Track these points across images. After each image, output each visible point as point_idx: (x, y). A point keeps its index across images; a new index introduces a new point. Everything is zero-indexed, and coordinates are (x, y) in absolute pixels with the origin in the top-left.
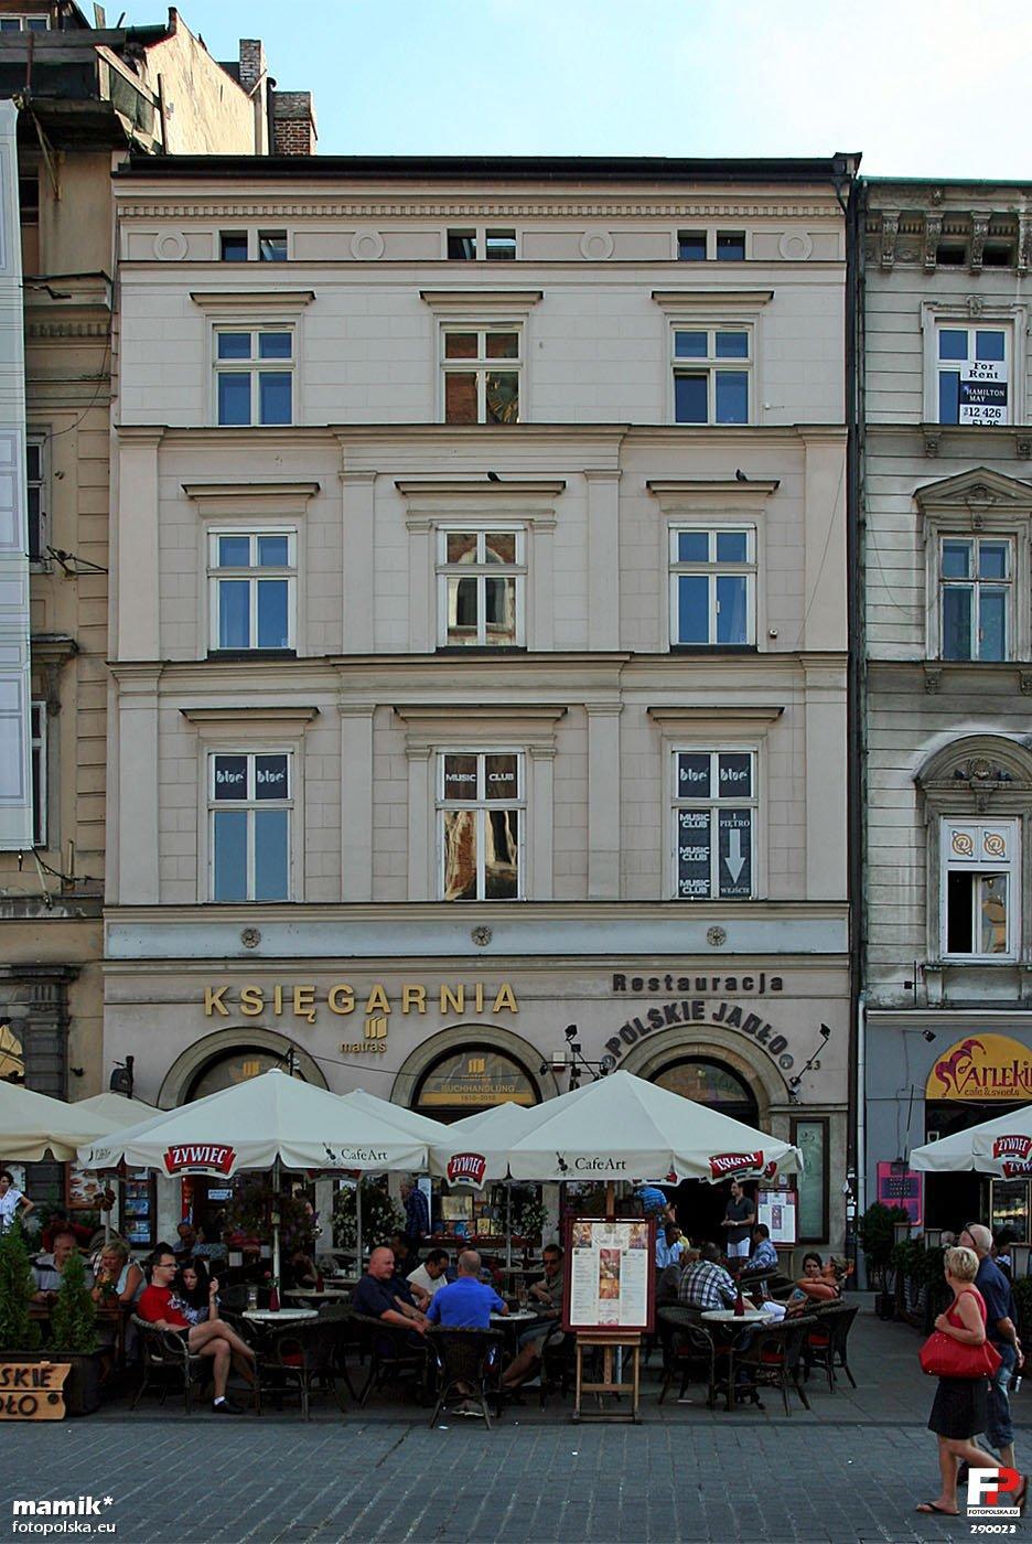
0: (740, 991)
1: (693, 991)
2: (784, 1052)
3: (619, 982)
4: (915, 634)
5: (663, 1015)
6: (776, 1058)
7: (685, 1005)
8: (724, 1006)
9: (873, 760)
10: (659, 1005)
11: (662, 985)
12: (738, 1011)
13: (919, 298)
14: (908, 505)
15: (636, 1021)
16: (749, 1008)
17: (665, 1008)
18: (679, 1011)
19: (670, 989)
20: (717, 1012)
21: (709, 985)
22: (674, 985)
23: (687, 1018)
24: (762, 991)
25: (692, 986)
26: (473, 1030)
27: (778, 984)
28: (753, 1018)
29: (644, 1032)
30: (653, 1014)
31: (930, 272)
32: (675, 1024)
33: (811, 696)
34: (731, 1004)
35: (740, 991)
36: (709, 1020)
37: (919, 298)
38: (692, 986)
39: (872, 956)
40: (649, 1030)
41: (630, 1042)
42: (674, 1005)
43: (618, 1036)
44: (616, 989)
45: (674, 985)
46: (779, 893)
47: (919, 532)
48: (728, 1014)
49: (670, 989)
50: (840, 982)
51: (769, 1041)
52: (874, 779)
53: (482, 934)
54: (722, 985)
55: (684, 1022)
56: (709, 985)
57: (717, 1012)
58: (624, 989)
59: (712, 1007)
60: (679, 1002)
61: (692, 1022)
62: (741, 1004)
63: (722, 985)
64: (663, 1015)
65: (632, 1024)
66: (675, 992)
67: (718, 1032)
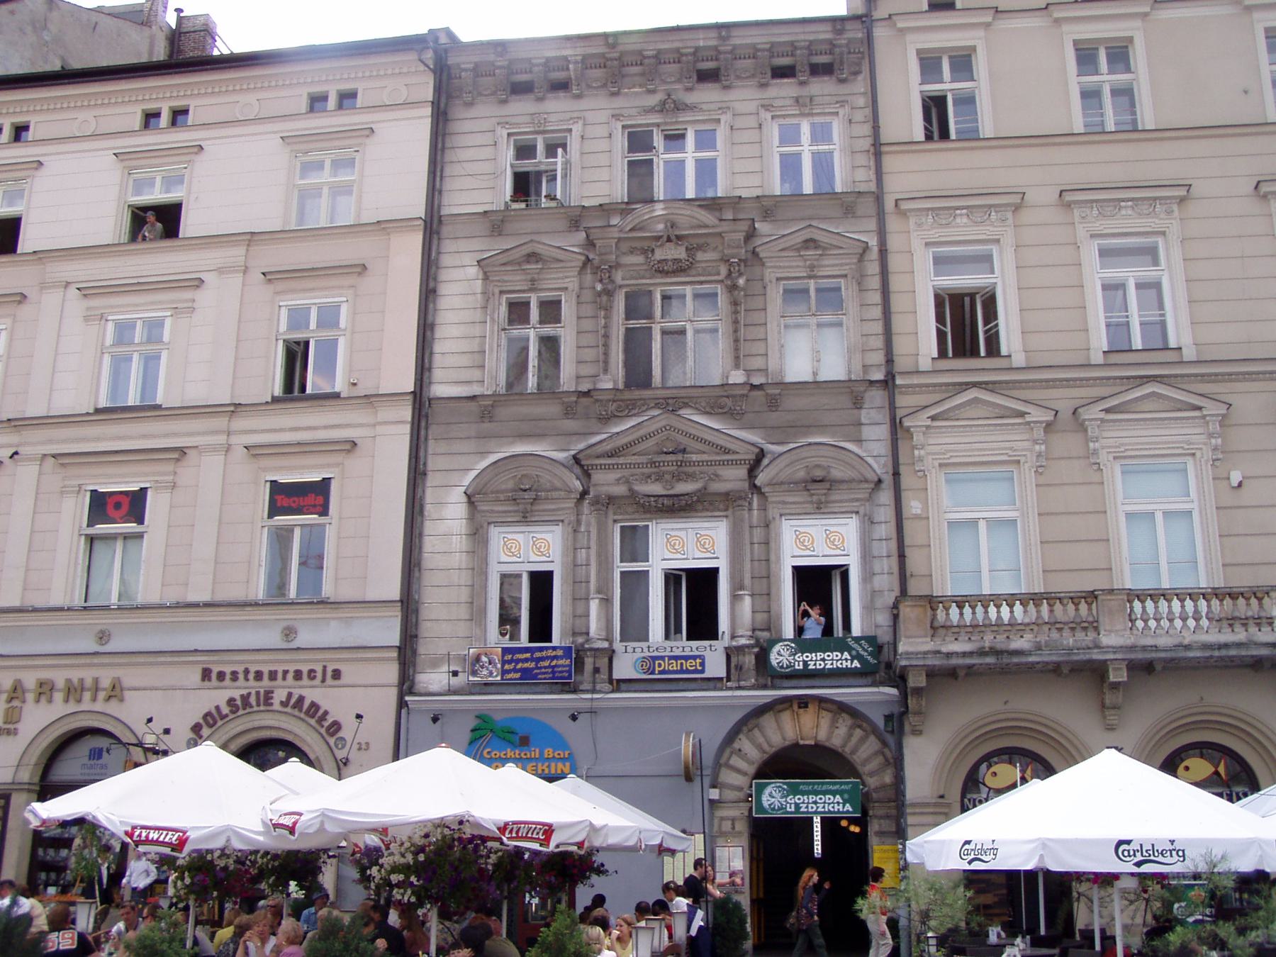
0: (305, 681)
1: (266, 682)
2: (340, 734)
3: (206, 674)
4: (476, 374)
5: (239, 702)
6: (332, 741)
7: (258, 693)
8: (290, 695)
9: (432, 480)
10: (236, 694)
11: (241, 676)
12: (301, 699)
13: (494, 120)
14: (473, 271)
15: (217, 708)
16: (313, 694)
17: (242, 696)
18: (253, 700)
19: (247, 679)
20: (284, 700)
21: (280, 675)
22: (251, 676)
23: (258, 705)
24: (324, 680)
25: (266, 676)
26: (88, 716)
27: (337, 674)
28: (314, 705)
29: (223, 717)
30: (231, 701)
31: (504, 102)
32: (248, 710)
33: (380, 429)
34: (297, 693)
35: (305, 681)
36: (277, 706)
37: (494, 120)
38: (266, 676)
39: (422, 649)
40: (226, 716)
41: (211, 726)
42: (249, 694)
43: (201, 721)
44: (203, 680)
45: (251, 676)
46: (347, 593)
47: (484, 293)
48: (293, 701)
49: (247, 679)
50: (391, 673)
51: (326, 724)
52: (430, 496)
53: (103, 637)
54: (290, 676)
55: (256, 709)
56: (280, 675)
57: (284, 700)
58: (210, 680)
59: (279, 696)
60: (253, 692)
61: (262, 708)
62: (304, 692)
63: (290, 676)
64: (239, 702)
65: (214, 711)
66: (252, 683)
67: (283, 718)
